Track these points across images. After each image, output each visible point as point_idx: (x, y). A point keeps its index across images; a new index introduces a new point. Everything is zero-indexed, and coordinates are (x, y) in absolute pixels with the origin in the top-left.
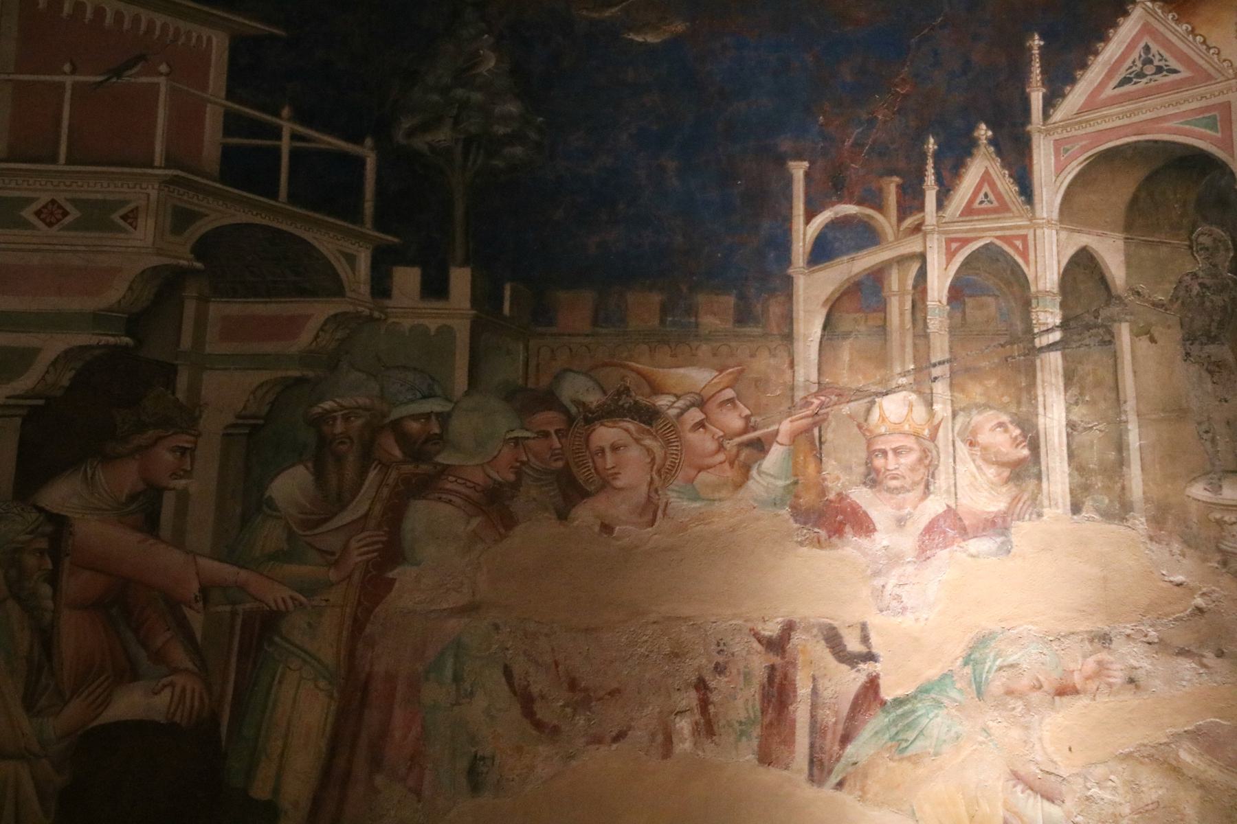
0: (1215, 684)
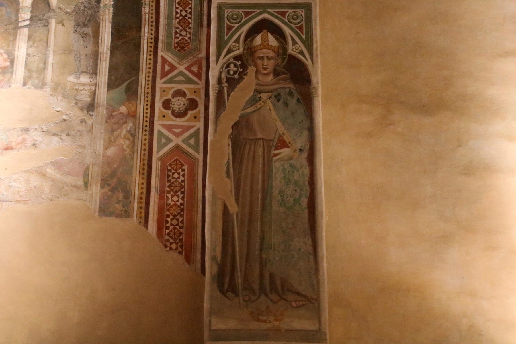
0: (64, 145)
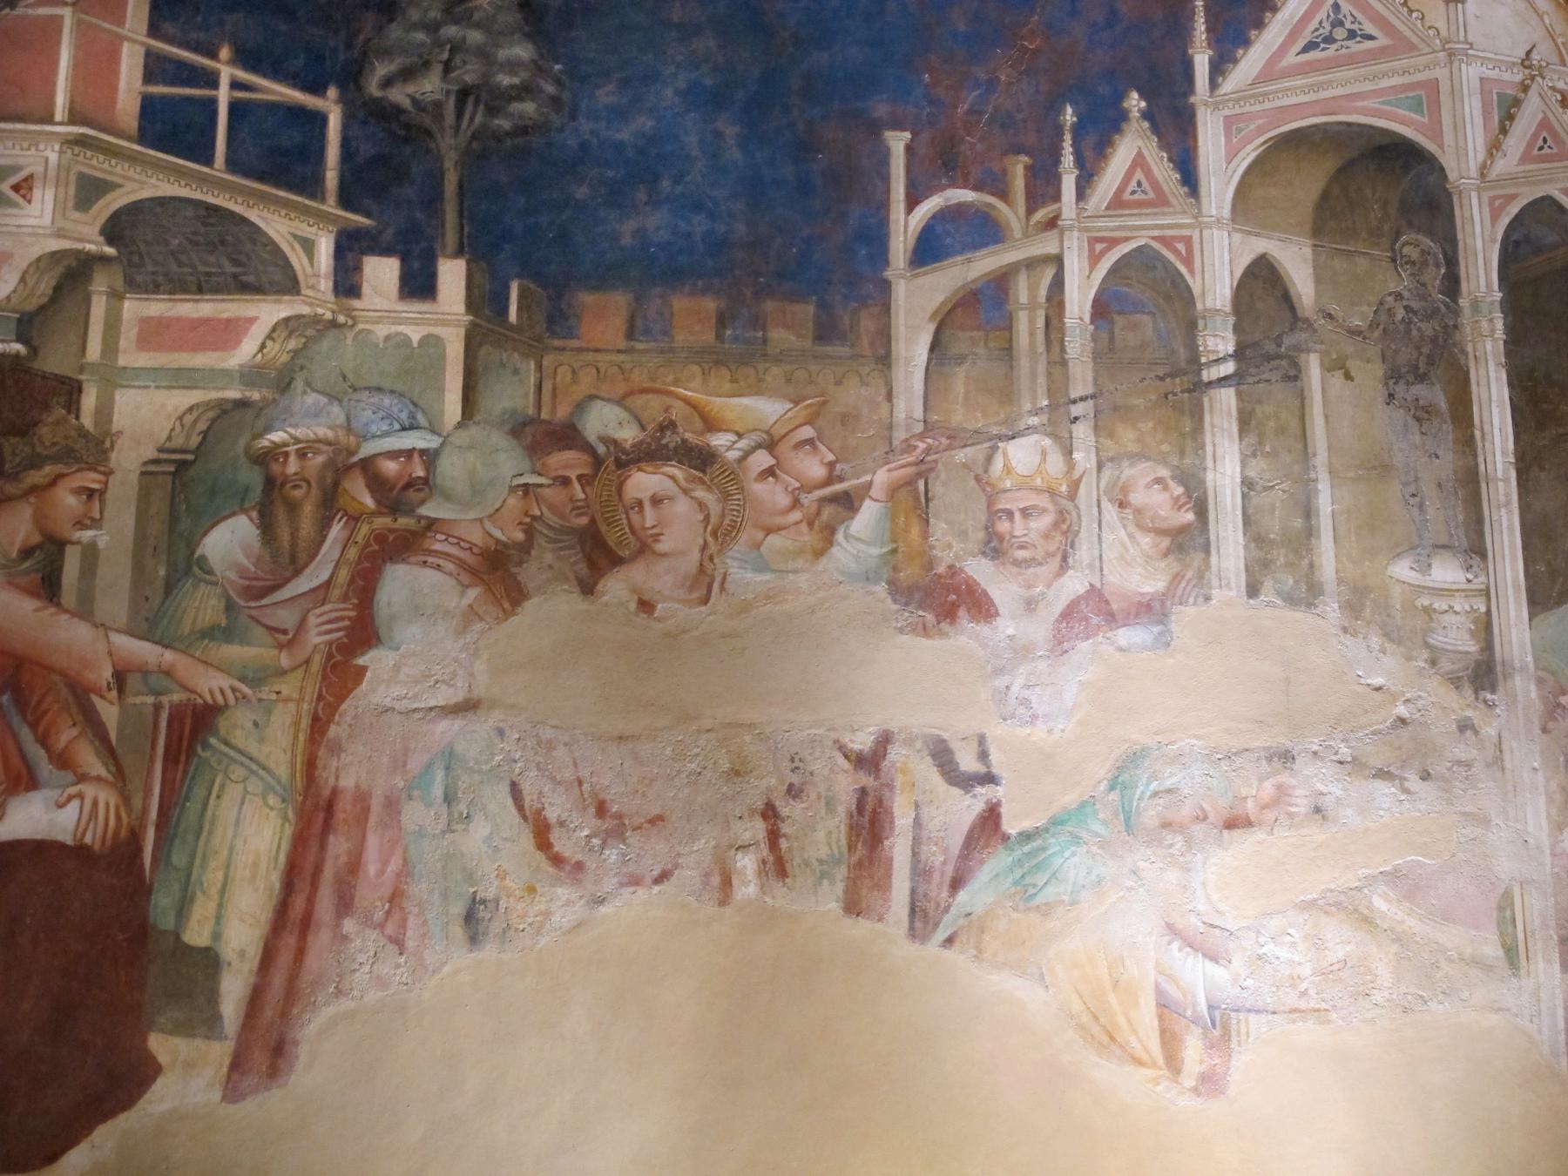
0: (1418, 814)
